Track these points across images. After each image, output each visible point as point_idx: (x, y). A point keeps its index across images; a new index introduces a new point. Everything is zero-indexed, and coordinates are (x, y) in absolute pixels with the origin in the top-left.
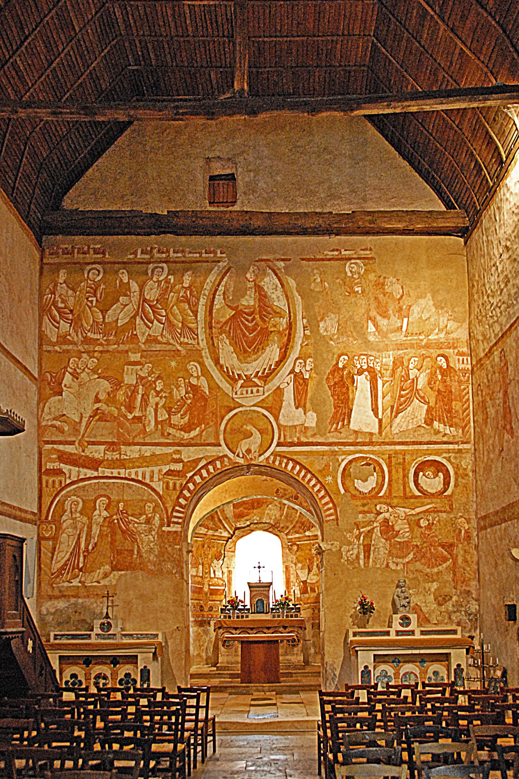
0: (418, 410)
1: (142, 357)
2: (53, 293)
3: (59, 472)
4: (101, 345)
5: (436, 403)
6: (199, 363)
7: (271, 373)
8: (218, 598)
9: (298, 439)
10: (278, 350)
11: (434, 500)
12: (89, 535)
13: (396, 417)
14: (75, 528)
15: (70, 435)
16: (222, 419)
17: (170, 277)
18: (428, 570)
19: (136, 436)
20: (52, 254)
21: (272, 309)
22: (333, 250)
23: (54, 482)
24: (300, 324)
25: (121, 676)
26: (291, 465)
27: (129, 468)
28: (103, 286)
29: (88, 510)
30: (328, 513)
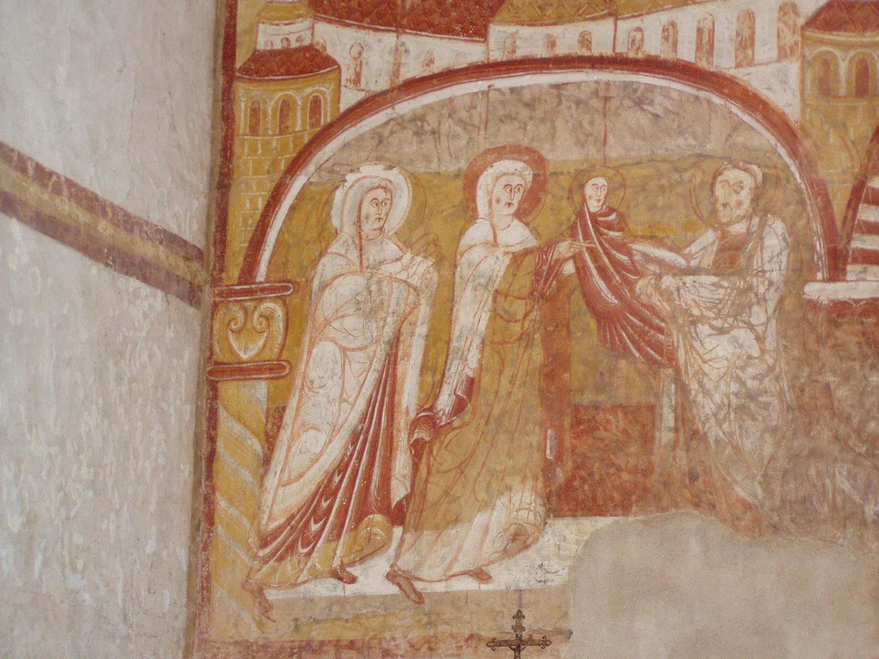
3: (309, 62)
12: (440, 339)
23: (285, 109)
27: (638, 12)
29: (440, 217)
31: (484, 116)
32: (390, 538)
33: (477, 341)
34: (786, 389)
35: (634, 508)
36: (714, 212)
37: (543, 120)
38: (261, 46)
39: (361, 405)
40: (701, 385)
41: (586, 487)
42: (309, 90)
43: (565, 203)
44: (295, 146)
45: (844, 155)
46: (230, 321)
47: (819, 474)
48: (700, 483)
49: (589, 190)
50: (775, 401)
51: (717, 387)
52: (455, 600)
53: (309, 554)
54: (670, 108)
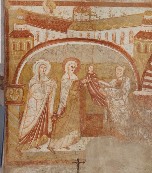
3: (26, 34)
12: (58, 99)
14: (44, 91)
23: (21, 44)
31: (66, 50)
32: (48, 140)
33: (66, 99)
34: (129, 112)
35: (99, 135)
36: (115, 75)
37: (80, 52)
38: (15, 29)
39: (41, 112)
40: (113, 111)
41: (89, 131)
42: (26, 41)
43: (84, 71)
44: (24, 53)
45: (142, 65)
46: (10, 92)
47: (136, 130)
48: (112, 131)
49: (89, 69)
50: (127, 115)
51: (116, 111)
53: (30, 143)
54: (107, 52)
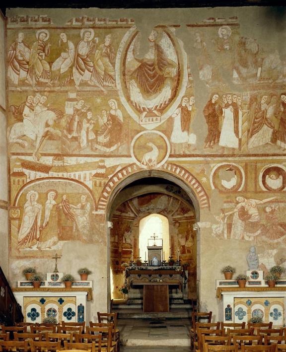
0: (266, 133)
1: (77, 95)
2: (15, 49)
3: (22, 174)
4: (49, 87)
5: (279, 127)
6: (116, 100)
7: (166, 107)
8: (128, 256)
9: (184, 152)
10: (171, 91)
11: (276, 194)
13: (251, 137)
15: (29, 149)
16: (132, 139)
17: (96, 39)
18: (271, 241)
19: (74, 150)
20: (13, 21)
21: (168, 62)
22: (210, 19)
23: (19, 181)
24: (186, 72)
25: (65, 309)
26: (178, 170)
28: (49, 45)
29: (42, 199)
30: (204, 202)
52: (46, 251)
